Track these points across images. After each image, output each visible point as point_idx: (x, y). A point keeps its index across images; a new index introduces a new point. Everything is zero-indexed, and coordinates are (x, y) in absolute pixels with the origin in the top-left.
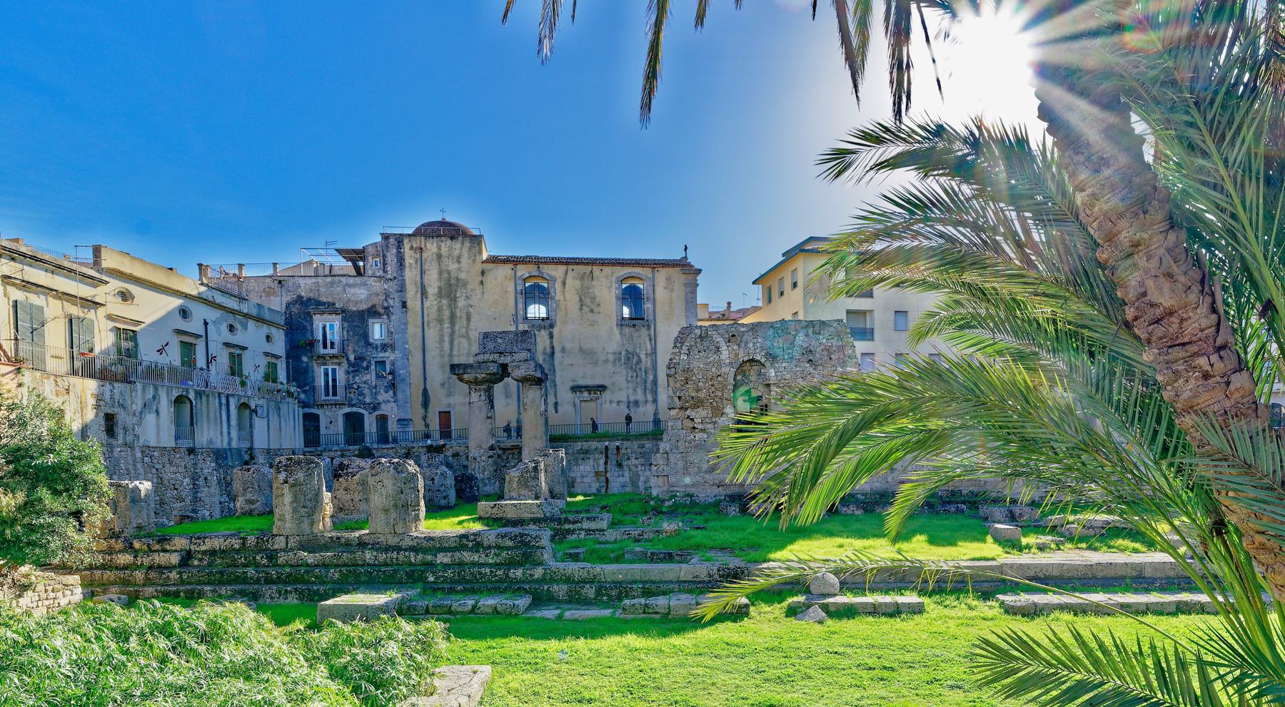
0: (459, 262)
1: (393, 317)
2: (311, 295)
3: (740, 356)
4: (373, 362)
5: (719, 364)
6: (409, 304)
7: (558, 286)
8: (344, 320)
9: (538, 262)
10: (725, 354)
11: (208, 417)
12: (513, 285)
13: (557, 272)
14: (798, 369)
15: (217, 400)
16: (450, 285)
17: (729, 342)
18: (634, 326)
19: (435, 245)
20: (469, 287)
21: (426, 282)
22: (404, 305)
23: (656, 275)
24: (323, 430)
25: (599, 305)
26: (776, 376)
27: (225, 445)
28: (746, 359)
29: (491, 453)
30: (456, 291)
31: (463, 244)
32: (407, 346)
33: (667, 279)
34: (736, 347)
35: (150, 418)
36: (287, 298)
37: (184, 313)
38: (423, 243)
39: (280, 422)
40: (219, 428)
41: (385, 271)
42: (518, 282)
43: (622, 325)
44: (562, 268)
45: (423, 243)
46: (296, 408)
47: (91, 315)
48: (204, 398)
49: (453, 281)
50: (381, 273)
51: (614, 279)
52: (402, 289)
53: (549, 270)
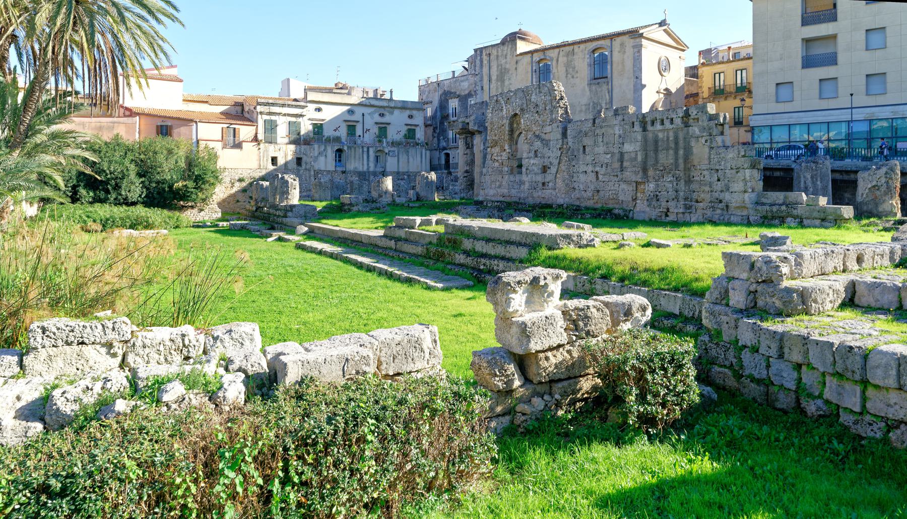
0: (506, 58)
1: (478, 96)
2: (449, 89)
5: (502, 117)
7: (554, 62)
8: (459, 101)
10: (504, 112)
11: (355, 157)
13: (553, 54)
15: (361, 150)
16: (501, 73)
18: (598, 83)
20: (510, 72)
23: (613, 43)
24: (451, 162)
25: (577, 72)
27: (365, 169)
29: (466, 175)
35: (322, 159)
36: (440, 92)
37: (351, 112)
39: (408, 159)
40: (361, 162)
42: (534, 64)
43: (591, 84)
44: (557, 50)
46: (424, 151)
47: (300, 120)
48: (353, 149)
50: (473, 72)
51: (586, 52)
52: (481, 80)
53: (551, 54)
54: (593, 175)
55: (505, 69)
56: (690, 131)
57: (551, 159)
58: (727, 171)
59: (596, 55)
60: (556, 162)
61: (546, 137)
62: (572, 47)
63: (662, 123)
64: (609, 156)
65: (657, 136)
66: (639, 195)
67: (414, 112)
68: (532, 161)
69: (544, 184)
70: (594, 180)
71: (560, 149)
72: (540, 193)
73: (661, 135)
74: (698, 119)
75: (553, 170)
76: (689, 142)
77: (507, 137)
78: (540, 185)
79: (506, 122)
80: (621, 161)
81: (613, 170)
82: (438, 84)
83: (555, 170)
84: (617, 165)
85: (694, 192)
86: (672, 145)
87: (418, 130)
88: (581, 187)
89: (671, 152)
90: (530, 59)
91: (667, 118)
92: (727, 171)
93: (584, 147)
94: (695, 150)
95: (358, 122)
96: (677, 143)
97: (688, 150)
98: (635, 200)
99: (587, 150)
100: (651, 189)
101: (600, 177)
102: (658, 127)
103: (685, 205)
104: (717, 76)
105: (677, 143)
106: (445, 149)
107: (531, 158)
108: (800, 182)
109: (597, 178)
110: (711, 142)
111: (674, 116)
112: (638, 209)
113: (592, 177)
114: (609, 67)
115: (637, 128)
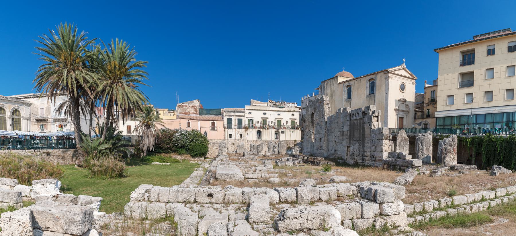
27: (270, 139)
58: (376, 141)
60: (323, 136)
64: (339, 133)
67: (294, 113)
69: (320, 147)
71: (325, 129)
73: (355, 122)
75: (323, 140)
77: (311, 124)
78: (319, 147)
79: (310, 116)
80: (343, 136)
84: (341, 137)
86: (359, 128)
87: (296, 121)
89: (358, 131)
92: (376, 141)
94: (366, 130)
95: (267, 118)
96: (360, 127)
102: (355, 118)
103: (362, 158)
105: (360, 127)
108: (417, 146)
111: (360, 112)
115: (348, 119)
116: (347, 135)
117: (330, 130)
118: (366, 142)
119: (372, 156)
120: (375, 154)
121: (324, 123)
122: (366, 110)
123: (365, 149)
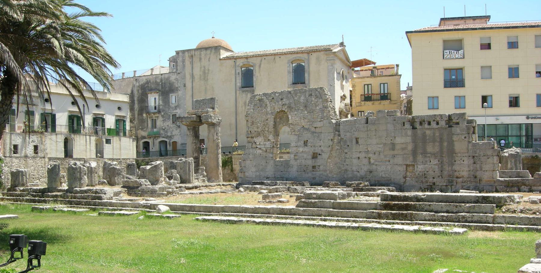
0: (209, 61)
3: (276, 109)
4: (171, 116)
5: (267, 113)
6: (187, 85)
7: (257, 68)
9: (247, 57)
10: (269, 109)
12: (235, 71)
13: (257, 61)
14: (302, 115)
16: (204, 73)
17: (271, 102)
19: (199, 53)
21: (195, 73)
22: (185, 86)
24: (151, 150)
26: (292, 119)
28: (278, 110)
30: (208, 76)
31: (211, 52)
32: (185, 106)
33: (317, 59)
34: (274, 104)
38: (193, 53)
41: (177, 70)
44: (259, 58)
45: (193, 53)
49: (207, 71)
50: (175, 71)
52: (184, 78)
54: (367, 160)
55: (209, 70)
56: (453, 131)
57: (322, 148)
59: (294, 65)
61: (318, 130)
62: (273, 57)
63: (429, 123)
65: (425, 133)
66: (408, 174)
68: (301, 149)
70: (367, 163)
72: (310, 175)
73: (428, 132)
74: (458, 124)
75: (325, 156)
76: (452, 137)
77: (271, 129)
78: (311, 168)
80: (393, 149)
81: (385, 156)
82: (136, 79)
83: (327, 156)
85: (456, 171)
86: (438, 140)
88: (354, 168)
89: (437, 144)
90: (233, 63)
91: (434, 121)
93: (357, 139)
97: (451, 143)
98: (405, 178)
99: (360, 141)
100: (420, 170)
101: (372, 161)
104: (382, 85)
106: (144, 137)
107: (300, 146)
109: (370, 162)
110: (469, 137)
112: (407, 184)
113: (365, 161)
114: (306, 75)
115: (408, 126)
116: (403, 149)
117: (351, 141)
118: (457, 159)
119: (472, 177)
120: (479, 174)
121: (331, 130)
122: (456, 118)
123: (456, 167)
